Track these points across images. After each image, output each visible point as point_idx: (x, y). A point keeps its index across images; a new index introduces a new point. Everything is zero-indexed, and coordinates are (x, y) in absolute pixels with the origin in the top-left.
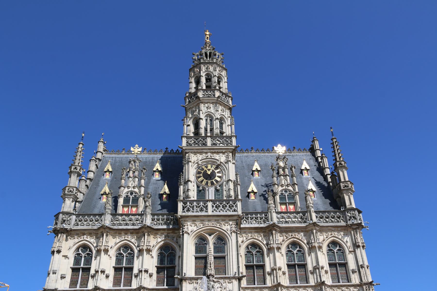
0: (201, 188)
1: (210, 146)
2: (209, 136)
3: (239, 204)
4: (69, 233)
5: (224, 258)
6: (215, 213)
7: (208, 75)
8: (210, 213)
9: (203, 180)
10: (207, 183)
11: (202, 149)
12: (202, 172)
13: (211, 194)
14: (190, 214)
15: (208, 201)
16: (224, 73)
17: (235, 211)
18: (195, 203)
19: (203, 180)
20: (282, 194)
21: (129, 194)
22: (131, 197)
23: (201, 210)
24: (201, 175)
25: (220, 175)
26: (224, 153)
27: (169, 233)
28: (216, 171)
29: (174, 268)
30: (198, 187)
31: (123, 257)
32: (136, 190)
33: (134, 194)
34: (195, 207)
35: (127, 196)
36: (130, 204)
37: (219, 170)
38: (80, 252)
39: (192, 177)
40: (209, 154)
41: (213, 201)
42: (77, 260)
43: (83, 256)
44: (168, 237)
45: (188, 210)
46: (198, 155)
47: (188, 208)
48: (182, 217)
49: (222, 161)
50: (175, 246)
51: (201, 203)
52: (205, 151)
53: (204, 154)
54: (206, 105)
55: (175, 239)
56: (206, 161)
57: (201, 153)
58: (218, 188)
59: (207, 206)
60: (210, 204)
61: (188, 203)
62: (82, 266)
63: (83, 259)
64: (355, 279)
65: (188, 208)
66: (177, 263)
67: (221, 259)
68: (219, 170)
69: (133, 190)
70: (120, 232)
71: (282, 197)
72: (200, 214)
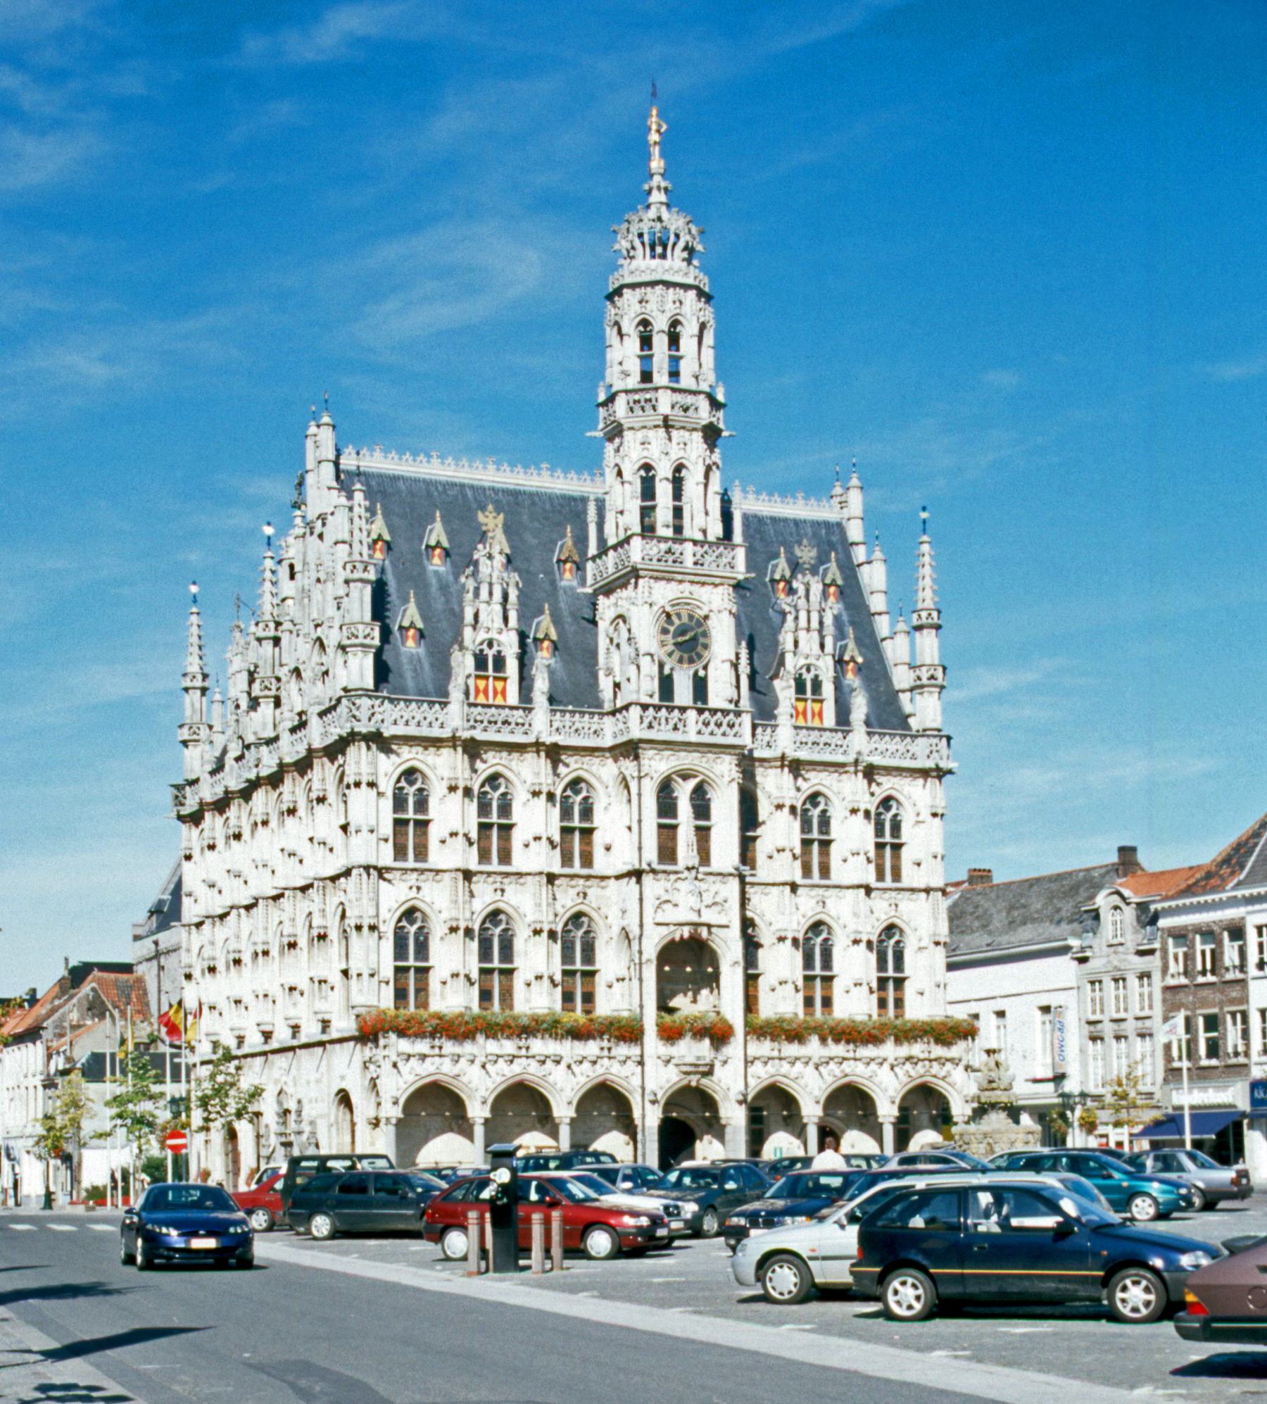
0: (667, 671)
8: (693, 738)
10: (680, 661)
22: (490, 653)
26: (716, 585)
33: (495, 648)
35: (481, 651)
41: (700, 711)
49: (714, 607)
52: (679, 577)
58: (701, 673)
67: (703, 834)
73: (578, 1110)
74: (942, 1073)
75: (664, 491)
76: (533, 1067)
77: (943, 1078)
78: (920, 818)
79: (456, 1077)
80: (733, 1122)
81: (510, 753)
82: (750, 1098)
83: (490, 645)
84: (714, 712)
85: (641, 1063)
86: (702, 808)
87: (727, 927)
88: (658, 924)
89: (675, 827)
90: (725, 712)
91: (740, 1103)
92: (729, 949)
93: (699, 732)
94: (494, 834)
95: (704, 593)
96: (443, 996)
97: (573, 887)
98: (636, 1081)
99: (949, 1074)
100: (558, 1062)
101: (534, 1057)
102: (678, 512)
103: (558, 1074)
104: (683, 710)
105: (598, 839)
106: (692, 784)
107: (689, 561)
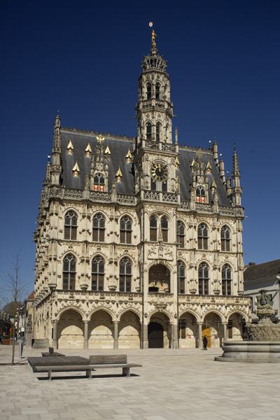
0: (154, 181)
3: (179, 197)
4: (61, 202)
5: (167, 230)
7: (158, 84)
8: (161, 201)
10: (158, 178)
13: (159, 187)
14: (149, 200)
16: (168, 83)
17: (176, 201)
26: (169, 157)
30: (152, 180)
32: (103, 173)
39: (149, 174)
42: (67, 221)
45: (147, 197)
48: (144, 201)
53: (156, 156)
54: (157, 113)
57: (154, 154)
67: (165, 232)
71: (198, 192)
72: (155, 201)
73: (92, 318)
75: (154, 130)
76: (105, 304)
79: (78, 307)
81: (104, 206)
83: (99, 175)
84: (168, 194)
85: (143, 304)
86: (164, 224)
89: (156, 229)
90: (172, 194)
91: (176, 318)
92: (173, 269)
93: (163, 200)
94: (99, 231)
95: (166, 159)
99: (244, 309)
100: (113, 303)
102: (158, 136)
104: (158, 193)
105: (133, 234)
106: (161, 216)
107: (161, 148)
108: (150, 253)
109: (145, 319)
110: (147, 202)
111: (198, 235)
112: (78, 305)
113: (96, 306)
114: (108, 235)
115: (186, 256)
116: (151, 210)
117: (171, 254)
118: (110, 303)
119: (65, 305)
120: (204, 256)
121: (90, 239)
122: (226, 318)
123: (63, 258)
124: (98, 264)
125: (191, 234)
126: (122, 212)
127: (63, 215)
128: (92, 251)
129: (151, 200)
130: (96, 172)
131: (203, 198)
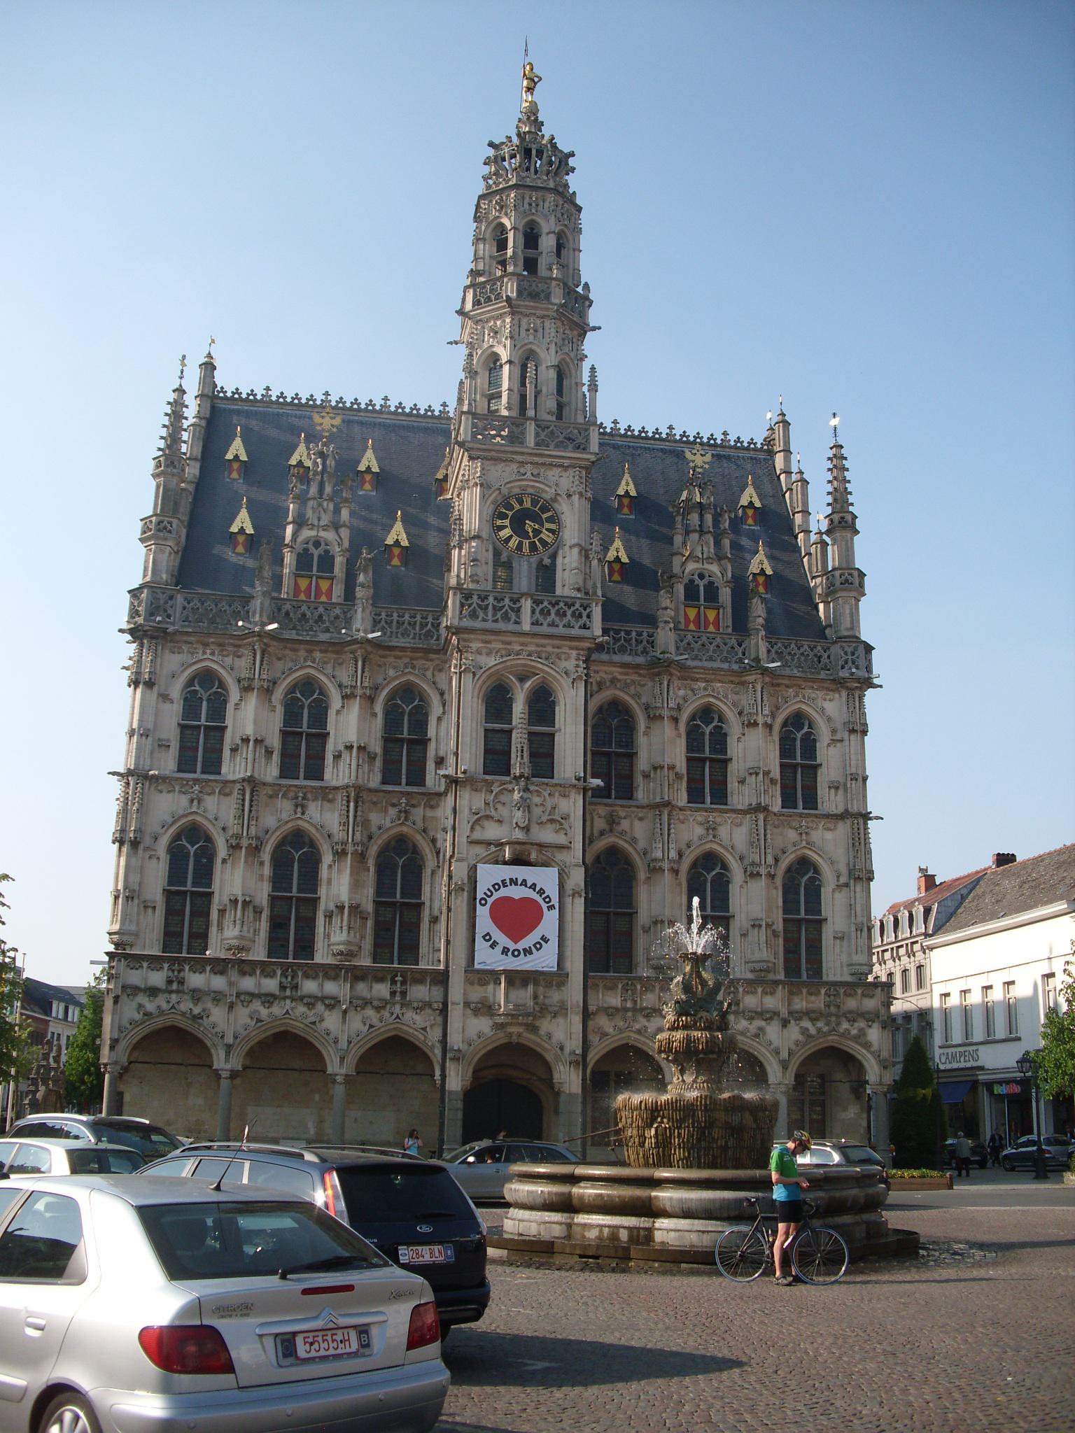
1: (532, 445)
2: (530, 419)
6: (537, 629)
8: (526, 627)
9: (511, 536)
11: (512, 453)
12: (510, 513)
14: (478, 624)
15: (523, 595)
17: (584, 627)
18: (491, 599)
19: (511, 536)
20: (692, 581)
21: (310, 546)
22: (316, 553)
23: (506, 618)
24: (507, 522)
25: (553, 526)
26: (566, 468)
27: (416, 659)
28: (544, 516)
29: (424, 742)
30: (497, 553)
31: (302, 707)
32: (329, 535)
33: (323, 546)
34: (490, 607)
35: (306, 550)
36: (315, 572)
37: (550, 514)
38: (197, 688)
40: (529, 469)
41: (537, 602)
43: (205, 698)
44: (414, 668)
46: (500, 466)
47: (474, 611)
50: (429, 691)
51: (507, 601)
52: (519, 458)
55: (429, 674)
56: (520, 487)
58: (547, 561)
59: (519, 610)
60: (527, 605)
61: (475, 597)
62: (203, 721)
63: (205, 704)
64: (830, 801)
65: (474, 611)
66: (431, 732)
68: (550, 514)
69: (322, 534)
70: (296, 646)
71: (691, 593)
72: (501, 626)
74: (854, 1032)
76: (301, 1009)
77: (856, 1039)
78: (838, 737)
80: (566, 1088)
82: (593, 1057)
85: (444, 1011)
87: (569, 848)
88: (471, 842)
89: (510, 732)
93: (535, 623)
94: (302, 745)
96: (220, 927)
97: (394, 805)
98: (435, 1035)
99: (862, 1033)
101: (302, 998)
103: (331, 1021)
107: (530, 440)
108: (479, 819)
109: (451, 1068)
110: (473, 631)
111: (690, 748)
112: (196, 1011)
113: (264, 1012)
114: (337, 757)
115: (636, 831)
116: (491, 661)
117: (560, 822)
118: (320, 1007)
119: (150, 1007)
120: (711, 829)
121: (271, 772)
122: (785, 1065)
123: (164, 841)
124: (295, 861)
125: (662, 747)
126: (391, 673)
127: (176, 691)
128: (276, 817)
129: (489, 625)
130: (306, 533)
131: (711, 615)
